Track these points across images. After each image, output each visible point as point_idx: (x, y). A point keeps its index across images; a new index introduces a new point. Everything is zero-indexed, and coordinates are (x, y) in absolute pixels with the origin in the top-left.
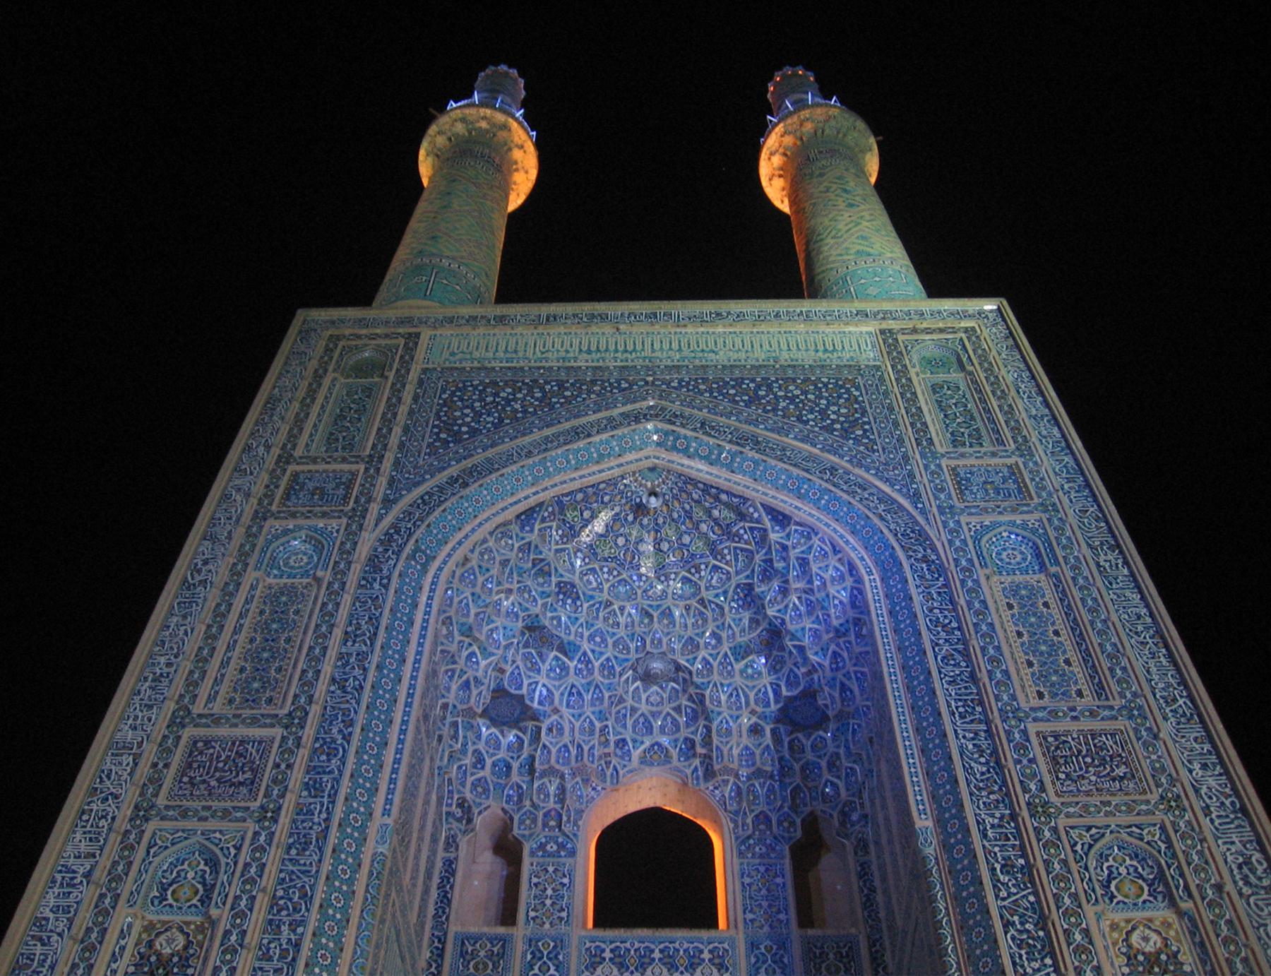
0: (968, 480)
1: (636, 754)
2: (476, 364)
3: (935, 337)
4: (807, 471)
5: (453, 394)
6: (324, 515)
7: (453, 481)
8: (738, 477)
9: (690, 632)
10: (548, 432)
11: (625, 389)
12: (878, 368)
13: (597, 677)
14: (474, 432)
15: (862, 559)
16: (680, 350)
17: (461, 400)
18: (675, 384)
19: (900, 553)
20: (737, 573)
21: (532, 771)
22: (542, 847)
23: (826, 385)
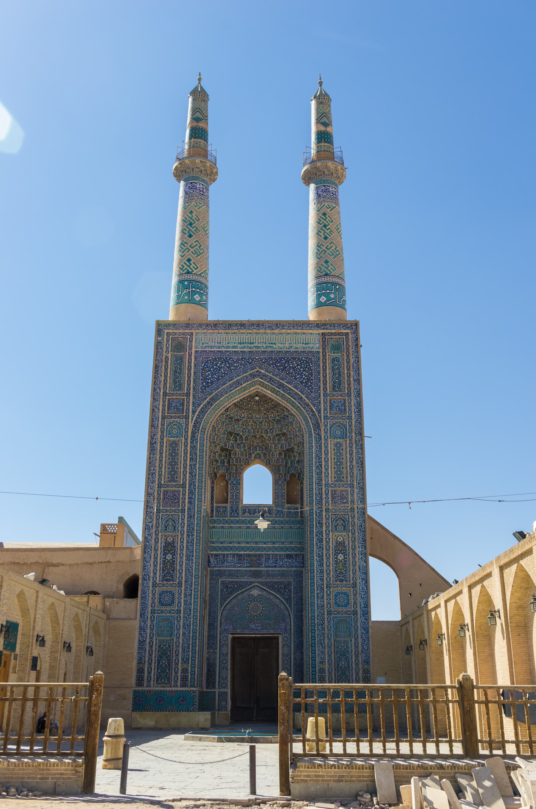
0: (333, 405)
1: (253, 456)
2: (210, 349)
3: (337, 337)
4: (295, 399)
5: (205, 365)
6: (179, 417)
7: (208, 403)
8: (278, 397)
9: (266, 428)
10: (231, 382)
11: (250, 363)
12: (319, 352)
13: (244, 441)
14: (212, 382)
15: (305, 429)
16: (266, 343)
17: (207, 367)
18: (263, 361)
19: (313, 431)
20: (278, 416)
21: (229, 463)
22: (232, 482)
23: (304, 361)
